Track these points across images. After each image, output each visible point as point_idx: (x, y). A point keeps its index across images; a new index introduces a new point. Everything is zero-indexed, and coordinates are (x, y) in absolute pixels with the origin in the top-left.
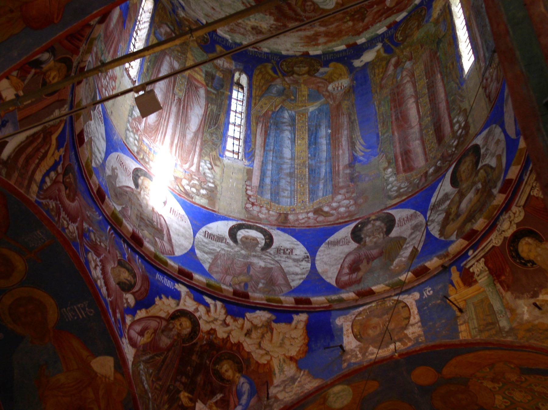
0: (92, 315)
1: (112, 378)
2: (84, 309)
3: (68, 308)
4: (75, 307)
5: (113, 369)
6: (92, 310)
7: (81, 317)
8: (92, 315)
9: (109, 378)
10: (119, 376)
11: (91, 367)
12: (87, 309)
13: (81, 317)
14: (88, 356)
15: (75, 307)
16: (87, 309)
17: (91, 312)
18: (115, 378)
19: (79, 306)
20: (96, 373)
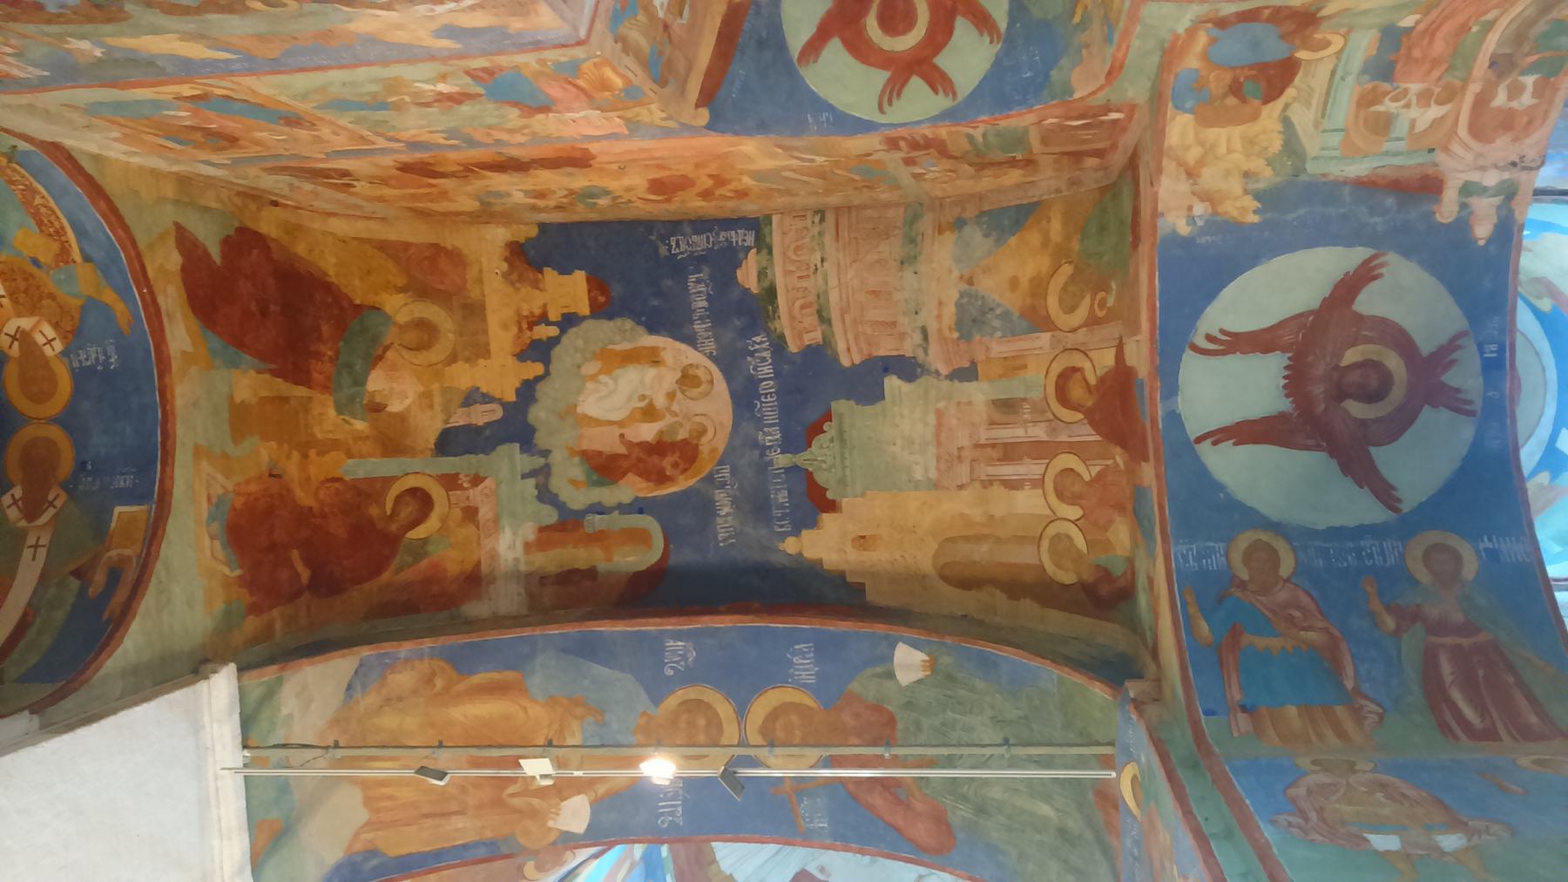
0: (659, 822)
1: (551, 824)
2: (671, 814)
3: (681, 792)
4: (680, 802)
5: (565, 828)
6: (666, 825)
7: (660, 804)
8: (659, 822)
9: (554, 819)
10: (552, 837)
11: (579, 794)
12: (671, 818)
13: (660, 804)
14: (596, 794)
15: (680, 802)
16: (671, 818)
17: (663, 822)
18: (550, 829)
19: (680, 809)
20: (565, 799)
